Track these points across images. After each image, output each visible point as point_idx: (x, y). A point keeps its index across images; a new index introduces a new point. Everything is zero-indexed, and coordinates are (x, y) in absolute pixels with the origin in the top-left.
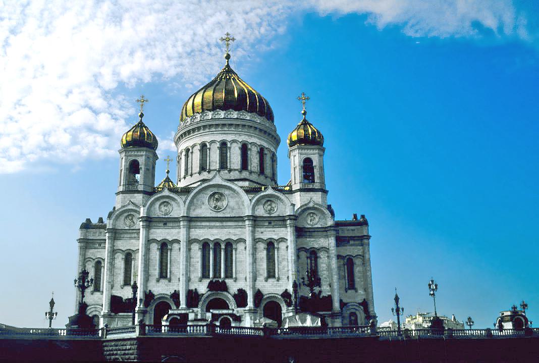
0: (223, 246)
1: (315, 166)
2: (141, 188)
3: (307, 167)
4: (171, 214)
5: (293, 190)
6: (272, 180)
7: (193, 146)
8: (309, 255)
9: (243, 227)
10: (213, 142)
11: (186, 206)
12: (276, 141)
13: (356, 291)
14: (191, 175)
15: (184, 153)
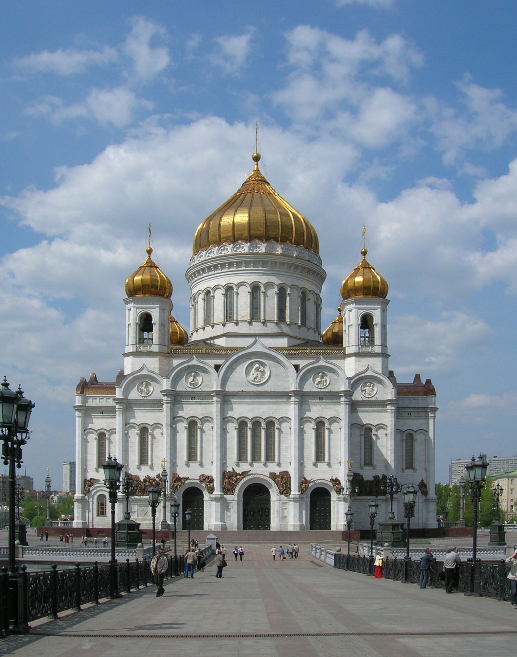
0: (263, 425)
1: (376, 325)
2: (155, 348)
3: (366, 322)
4: (201, 387)
5: (347, 353)
6: (315, 332)
7: (216, 288)
8: (363, 433)
9: (287, 403)
10: (241, 284)
11: (220, 378)
12: (320, 277)
13: (415, 472)
14: (213, 327)
15: (202, 296)
